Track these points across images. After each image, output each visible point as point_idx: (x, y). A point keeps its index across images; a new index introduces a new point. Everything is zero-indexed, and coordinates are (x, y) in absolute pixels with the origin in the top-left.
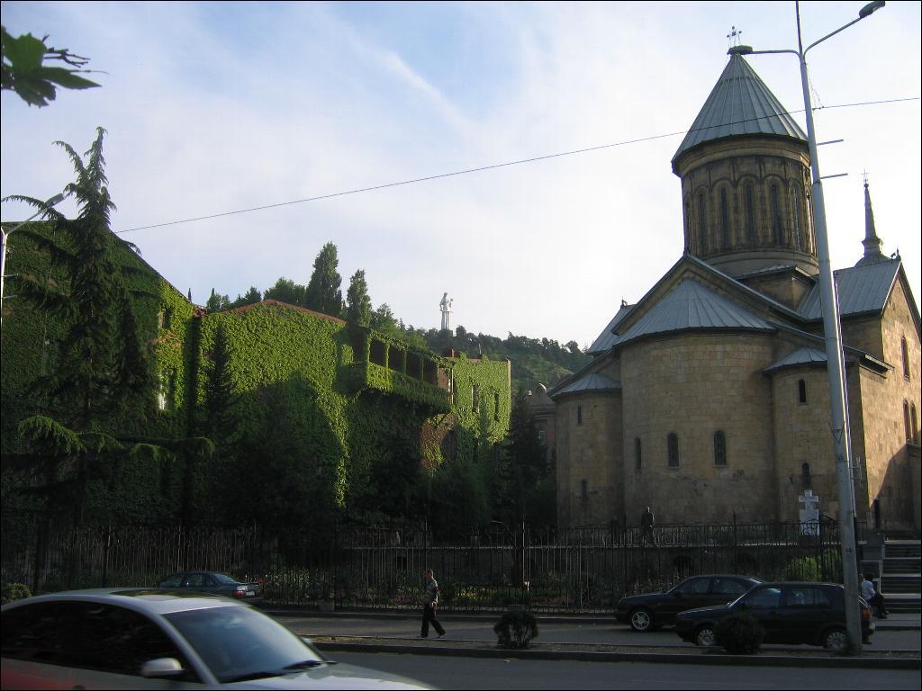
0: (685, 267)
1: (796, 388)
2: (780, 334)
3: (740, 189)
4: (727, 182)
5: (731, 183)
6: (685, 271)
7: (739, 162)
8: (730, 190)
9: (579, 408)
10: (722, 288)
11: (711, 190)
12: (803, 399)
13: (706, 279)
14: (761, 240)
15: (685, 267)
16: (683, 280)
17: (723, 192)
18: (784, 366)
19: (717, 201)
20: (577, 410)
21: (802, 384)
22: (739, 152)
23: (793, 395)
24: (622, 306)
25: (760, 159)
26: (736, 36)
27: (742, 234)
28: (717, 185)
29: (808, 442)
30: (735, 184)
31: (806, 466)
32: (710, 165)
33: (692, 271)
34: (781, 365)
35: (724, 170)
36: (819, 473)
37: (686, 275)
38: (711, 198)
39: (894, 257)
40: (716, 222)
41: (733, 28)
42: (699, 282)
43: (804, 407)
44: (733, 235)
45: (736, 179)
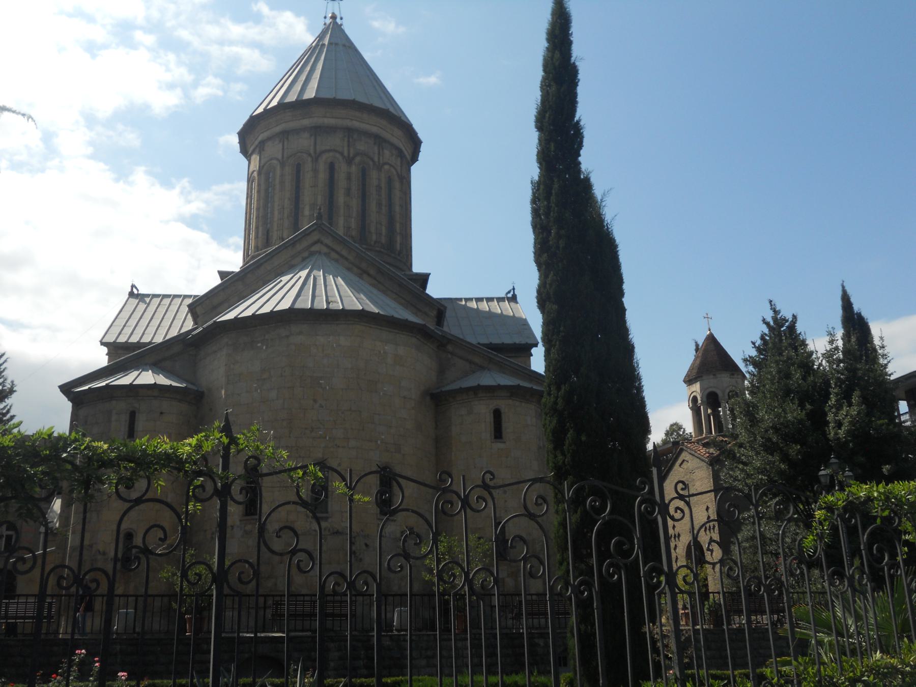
0: (315, 236)
1: (490, 418)
2: (450, 348)
3: (354, 169)
4: (338, 155)
5: (344, 157)
6: (315, 243)
8: (342, 169)
9: (133, 415)
10: (369, 275)
11: (316, 159)
12: (498, 433)
13: (346, 259)
14: (374, 237)
15: (315, 236)
16: (312, 254)
17: (332, 168)
18: (461, 388)
19: (323, 176)
20: (125, 418)
21: (497, 414)
23: (485, 428)
24: (131, 294)
25: (379, 140)
27: (353, 223)
28: (325, 156)
30: (349, 161)
33: (327, 246)
34: (458, 387)
37: (314, 249)
38: (315, 171)
39: (510, 295)
42: (337, 261)
43: (500, 445)
44: (341, 221)
45: (351, 155)
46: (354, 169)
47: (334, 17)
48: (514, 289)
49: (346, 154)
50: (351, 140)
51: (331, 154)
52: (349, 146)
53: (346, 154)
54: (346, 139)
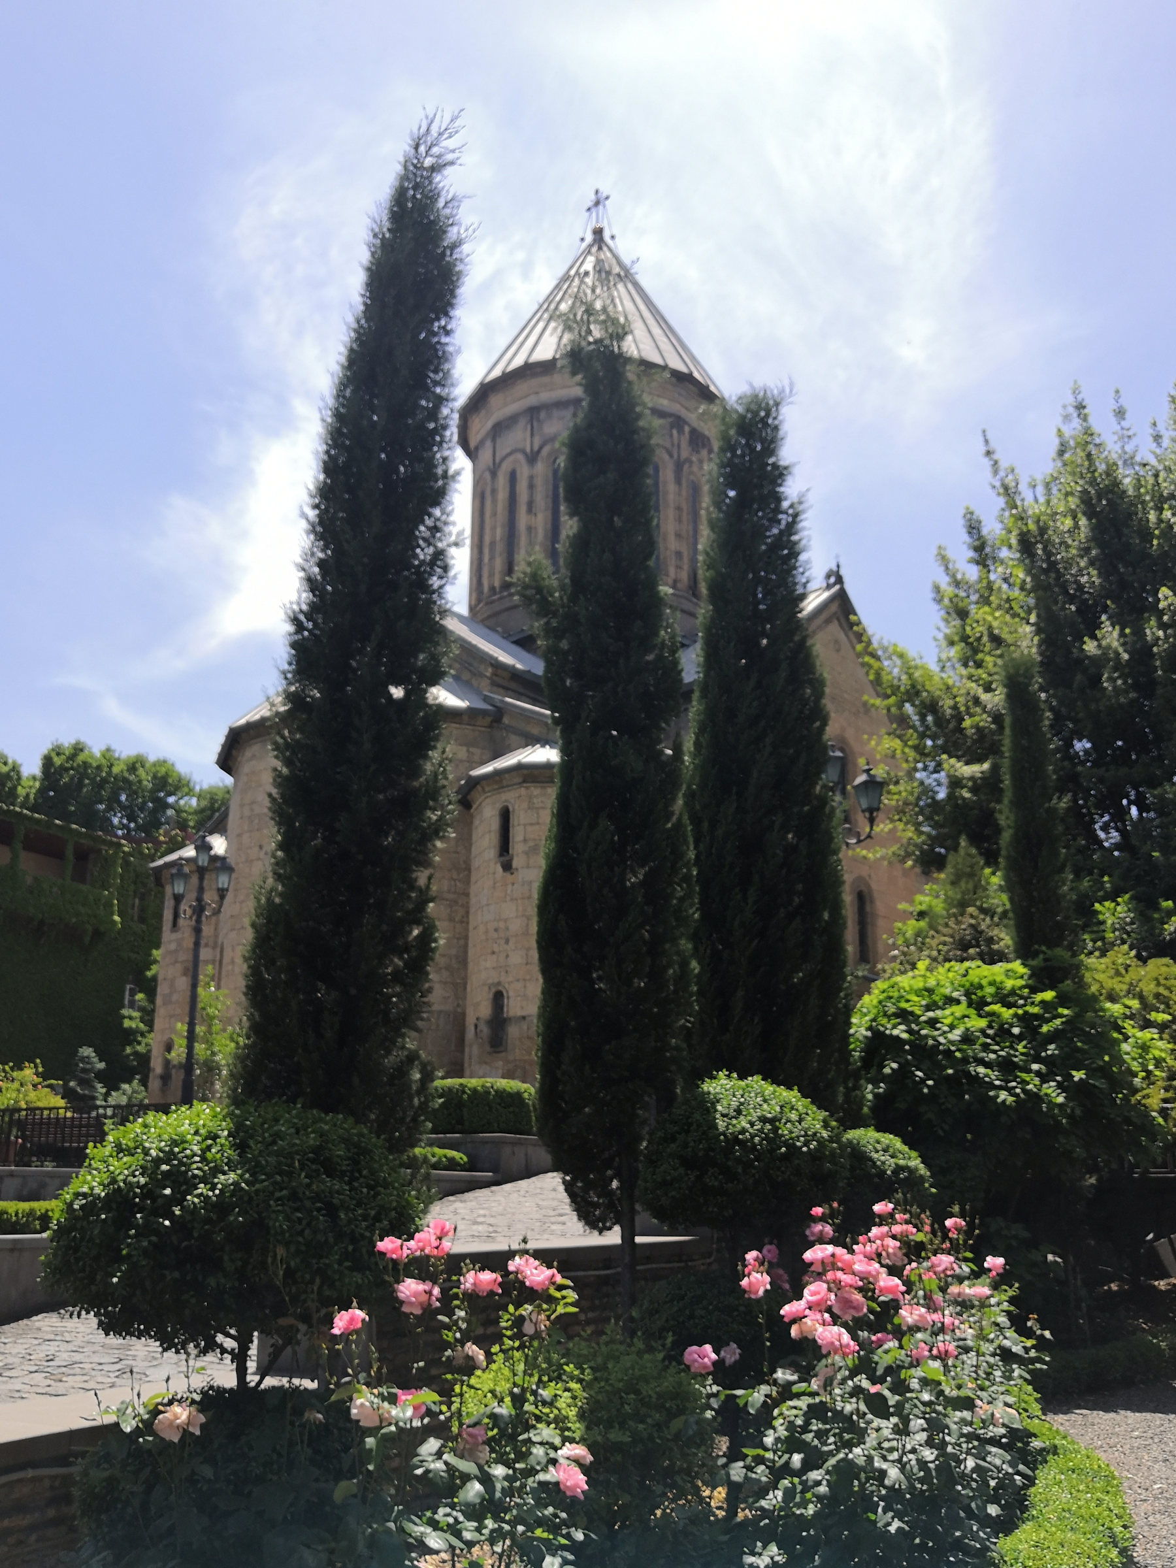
3: (540, 467)
7: (543, 415)
8: (524, 472)
17: (513, 477)
21: (505, 816)
22: (546, 396)
26: (601, 207)
29: (507, 942)
30: (532, 458)
31: (498, 998)
32: (498, 430)
35: (518, 437)
36: (520, 1013)
40: (498, 538)
41: (597, 192)
45: (536, 448)
46: (540, 467)
47: (598, 233)
48: (838, 566)
49: (528, 450)
50: (535, 424)
51: (511, 458)
52: (532, 435)
53: (528, 450)
54: (529, 427)
